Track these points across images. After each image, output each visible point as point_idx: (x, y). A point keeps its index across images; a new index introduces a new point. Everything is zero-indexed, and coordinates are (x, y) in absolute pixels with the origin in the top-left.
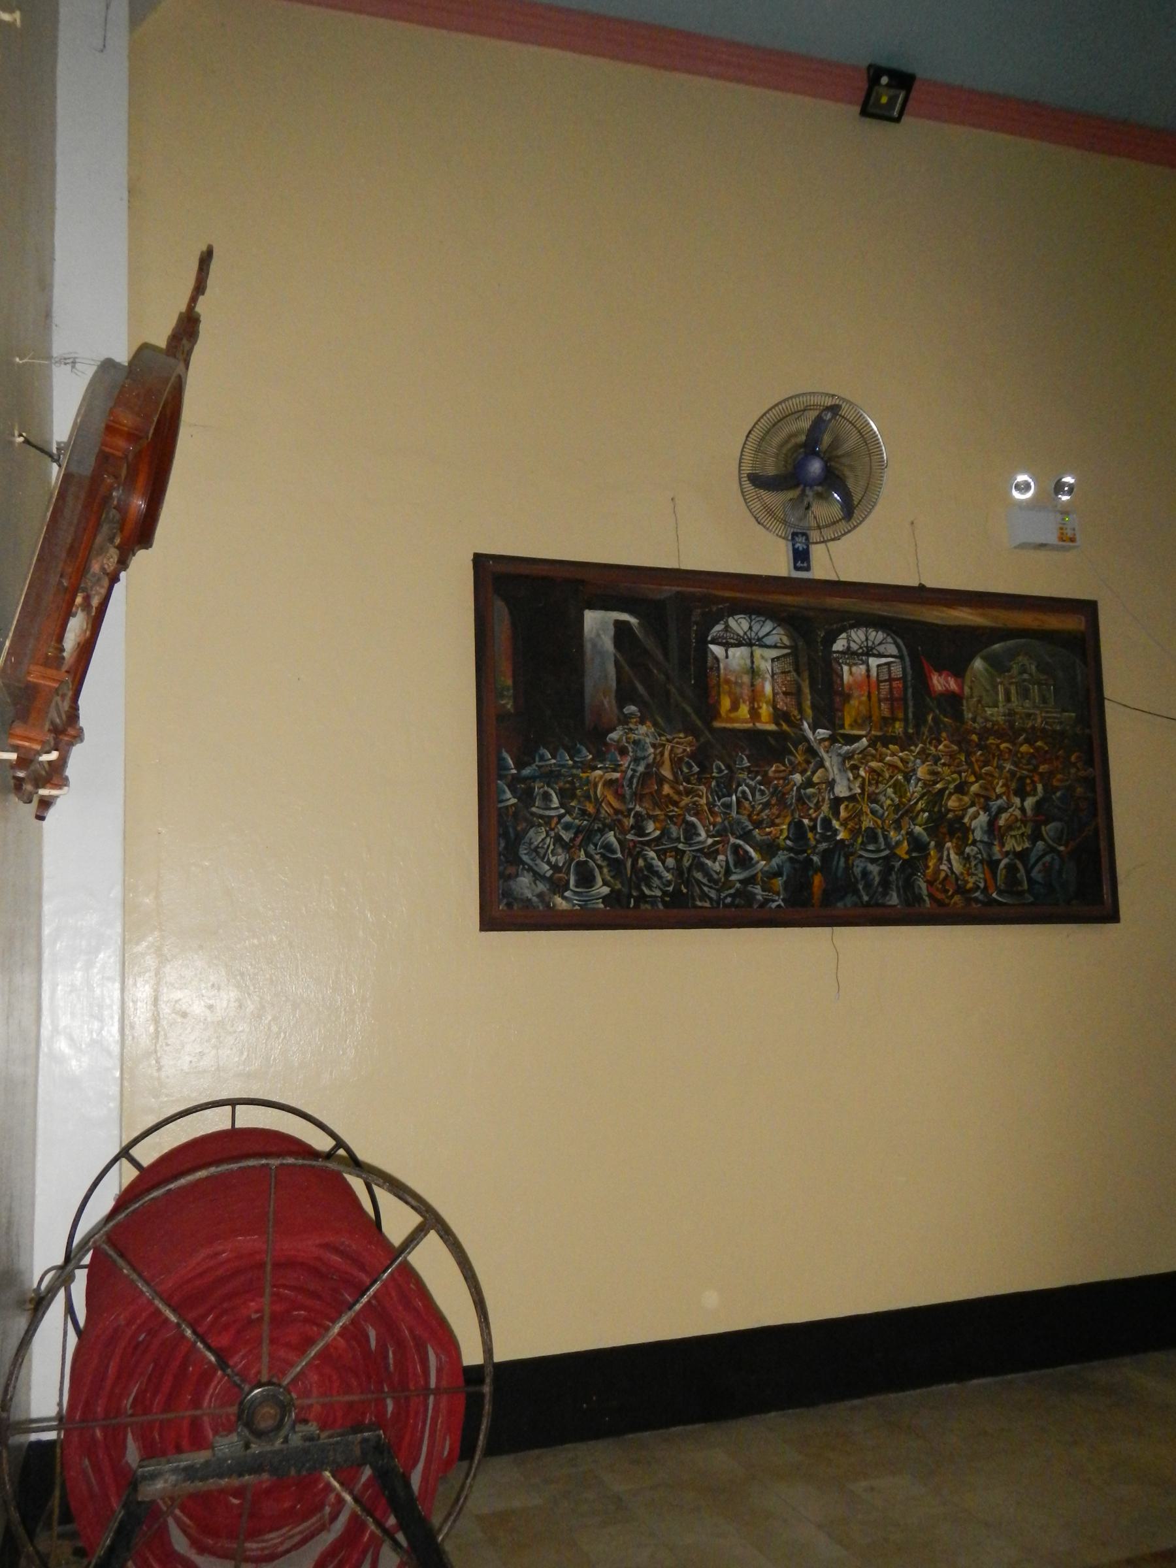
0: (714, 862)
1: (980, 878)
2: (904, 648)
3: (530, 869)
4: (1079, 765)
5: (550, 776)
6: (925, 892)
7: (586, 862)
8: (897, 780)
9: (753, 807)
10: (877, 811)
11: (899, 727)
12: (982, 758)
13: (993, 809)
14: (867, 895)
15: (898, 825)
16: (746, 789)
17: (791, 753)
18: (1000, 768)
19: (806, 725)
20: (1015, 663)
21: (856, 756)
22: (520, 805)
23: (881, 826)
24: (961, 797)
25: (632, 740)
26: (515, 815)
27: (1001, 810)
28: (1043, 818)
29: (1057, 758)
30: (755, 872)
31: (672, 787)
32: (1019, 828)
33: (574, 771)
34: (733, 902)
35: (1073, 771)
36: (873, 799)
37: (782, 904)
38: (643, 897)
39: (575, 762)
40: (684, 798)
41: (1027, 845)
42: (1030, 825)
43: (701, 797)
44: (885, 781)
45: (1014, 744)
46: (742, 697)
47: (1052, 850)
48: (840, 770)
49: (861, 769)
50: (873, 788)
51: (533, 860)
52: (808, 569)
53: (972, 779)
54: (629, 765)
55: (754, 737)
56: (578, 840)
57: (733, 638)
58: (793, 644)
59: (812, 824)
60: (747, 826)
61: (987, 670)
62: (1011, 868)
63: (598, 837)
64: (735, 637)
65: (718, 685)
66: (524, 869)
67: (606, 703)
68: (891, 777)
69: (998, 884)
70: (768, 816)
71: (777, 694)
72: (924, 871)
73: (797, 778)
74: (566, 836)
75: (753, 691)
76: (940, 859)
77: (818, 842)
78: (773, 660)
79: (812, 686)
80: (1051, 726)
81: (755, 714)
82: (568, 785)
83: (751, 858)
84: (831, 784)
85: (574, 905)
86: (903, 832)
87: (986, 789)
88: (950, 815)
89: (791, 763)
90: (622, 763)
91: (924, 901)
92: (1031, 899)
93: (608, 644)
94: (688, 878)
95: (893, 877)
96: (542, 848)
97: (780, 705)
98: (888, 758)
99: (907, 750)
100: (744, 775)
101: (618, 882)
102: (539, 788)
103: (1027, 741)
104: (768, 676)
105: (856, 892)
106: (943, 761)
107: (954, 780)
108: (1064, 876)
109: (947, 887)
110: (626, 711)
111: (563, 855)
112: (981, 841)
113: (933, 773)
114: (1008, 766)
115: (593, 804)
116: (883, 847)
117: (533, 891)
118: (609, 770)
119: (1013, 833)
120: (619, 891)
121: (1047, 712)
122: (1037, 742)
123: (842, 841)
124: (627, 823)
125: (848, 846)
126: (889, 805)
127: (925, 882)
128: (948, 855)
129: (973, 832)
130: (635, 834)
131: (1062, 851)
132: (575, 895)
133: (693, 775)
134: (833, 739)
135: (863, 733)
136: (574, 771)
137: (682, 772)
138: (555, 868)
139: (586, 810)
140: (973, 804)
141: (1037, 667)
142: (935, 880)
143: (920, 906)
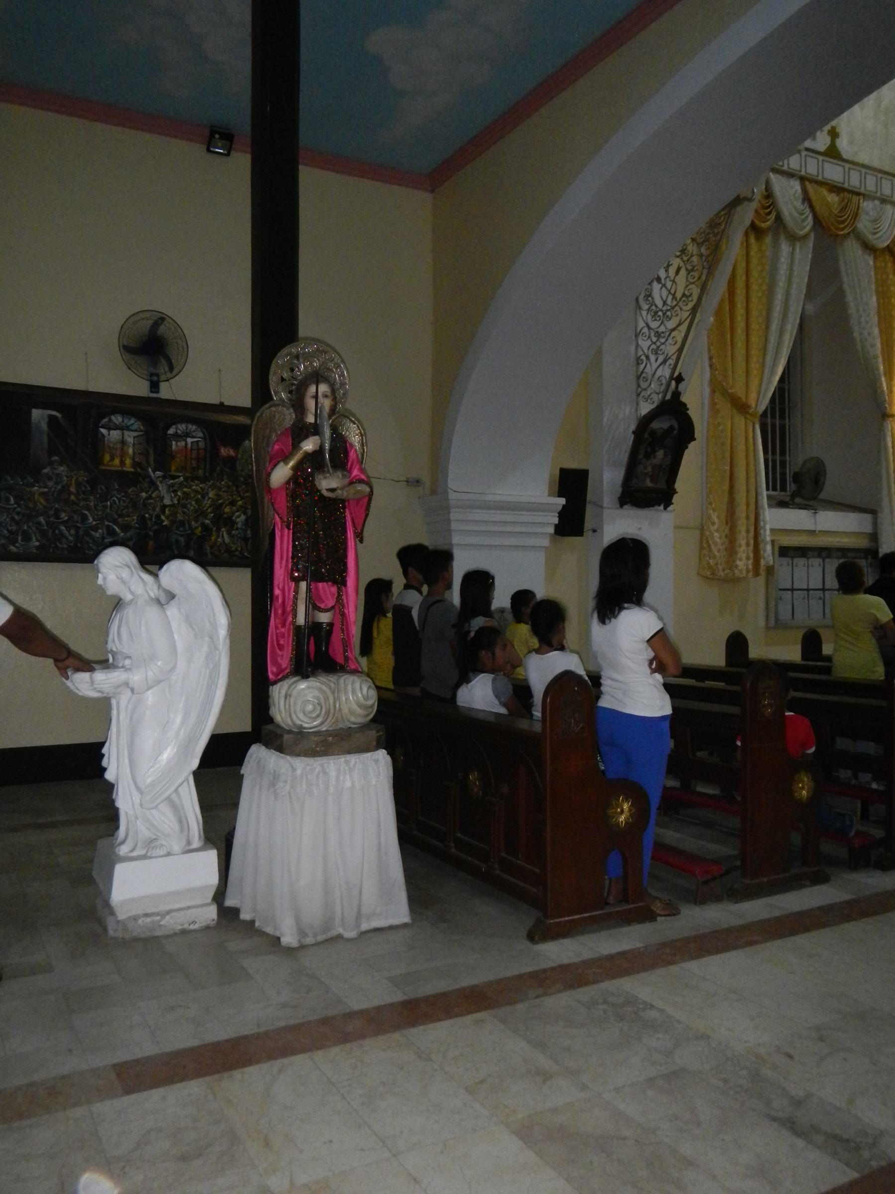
11: (201, 472)
16: (116, 499)
19: (150, 470)
21: (176, 486)
31: (76, 497)
33: (23, 487)
36: (184, 506)
43: (90, 502)
50: (184, 501)
52: (158, 392)
53: (239, 499)
55: (121, 475)
68: (195, 496)
73: (144, 495)
74: (16, 517)
78: (134, 437)
81: (122, 463)
84: (162, 499)
85: (20, 550)
88: (225, 516)
93: (44, 426)
97: (137, 459)
98: (194, 487)
100: (115, 492)
107: (229, 499)
113: (217, 495)
123: (166, 525)
128: (223, 535)
129: (237, 524)
134: (164, 477)
135: (181, 474)
138: (11, 532)
140: (238, 511)
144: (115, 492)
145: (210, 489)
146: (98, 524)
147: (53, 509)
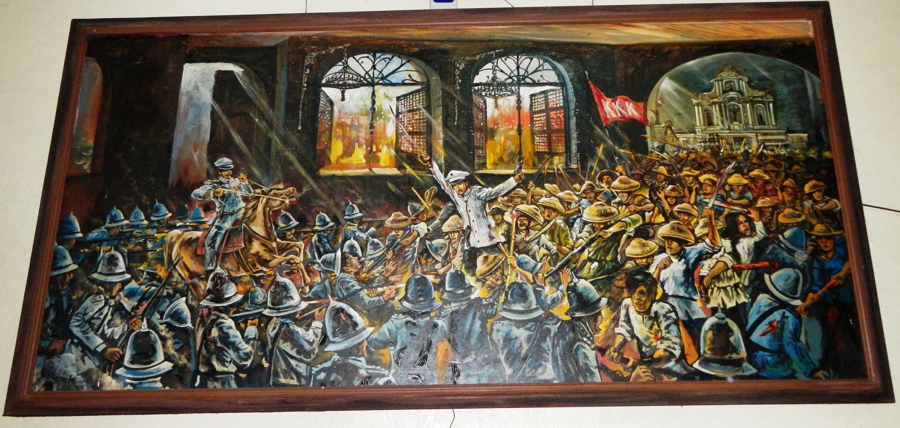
0: (307, 330)
1: (676, 343)
2: (565, 74)
3: (80, 343)
4: (816, 195)
5: (119, 239)
6: (593, 363)
8: (555, 225)
9: (362, 263)
11: (558, 163)
12: (673, 194)
13: (690, 256)
17: (419, 201)
18: (699, 204)
19: (436, 168)
20: (718, 81)
21: (500, 199)
22: (81, 271)
23: (532, 281)
24: (644, 241)
25: (221, 194)
26: (73, 281)
27: (702, 257)
28: (767, 263)
29: (783, 188)
30: (360, 341)
31: (263, 245)
32: (730, 279)
35: (808, 204)
36: (522, 248)
38: (212, 374)
39: (151, 222)
41: (743, 299)
43: (297, 254)
44: (539, 227)
45: (719, 174)
46: (358, 141)
47: (783, 305)
48: (478, 216)
51: (84, 332)
53: (661, 219)
56: (142, 309)
57: (352, 79)
58: (425, 80)
59: (438, 281)
60: (353, 286)
61: (677, 91)
62: (721, 330)
63: (166, 305)
64: (355, 77)
65: (330, 129)
66: (72, 343)
67: (195, 157)
68: (547, 222)
69: (702, 351)
70: (381, 273)
71: (402, 134)
73: (422, 228)
74: (128, 304)
75: (372, 133)
76: (616, 320)
78: (398, 99)
79: (446, 125)
80: (772, 150)
81: (372, 158)
82: (139, 247)
83: (355, 324)
84: (466, 233)
85: (126, 385)
87: (680, 231)
88: (629, 265)
89: (414, 210)
91: (592, 373)
92: (754, 371)
93: (206, 96)
95: (548, 344)
98: (543, 199)
99: (570, 189)
101: (183, 356)
103: (738, 170)
104: (392, 117)
106: (618, 199)
107: (634, 222)
109: (625, 356)
110: (217, 164)
111: (121, 326)
114: (712, 202)
115: (166, 267)
116: (534, 306)
117: (78, 370)
118: (190, 228)
119: (721, 285)
120: (185, 366)
121: (765, 134)
122: (752, 171)
123: (479, 300)
124: (203, 287)
125: (486, 306)
126: (544, 255)
127: (593, 349)
128: (627, 315)
129: (662, 286)
130: (212, 300)
131: (797, 306)
132: (128, 373)
133: (290, 230)
134: (470, 181)
135: (511, 172)
137: (277, 226)
138: (110, 341)
139: (156, 274)
140: (662, 250)
141: (749, 83)
142: (609, 347)
144: (354, 228)
145: (584, 201)
146: (314, 306)
147: (211, 276)
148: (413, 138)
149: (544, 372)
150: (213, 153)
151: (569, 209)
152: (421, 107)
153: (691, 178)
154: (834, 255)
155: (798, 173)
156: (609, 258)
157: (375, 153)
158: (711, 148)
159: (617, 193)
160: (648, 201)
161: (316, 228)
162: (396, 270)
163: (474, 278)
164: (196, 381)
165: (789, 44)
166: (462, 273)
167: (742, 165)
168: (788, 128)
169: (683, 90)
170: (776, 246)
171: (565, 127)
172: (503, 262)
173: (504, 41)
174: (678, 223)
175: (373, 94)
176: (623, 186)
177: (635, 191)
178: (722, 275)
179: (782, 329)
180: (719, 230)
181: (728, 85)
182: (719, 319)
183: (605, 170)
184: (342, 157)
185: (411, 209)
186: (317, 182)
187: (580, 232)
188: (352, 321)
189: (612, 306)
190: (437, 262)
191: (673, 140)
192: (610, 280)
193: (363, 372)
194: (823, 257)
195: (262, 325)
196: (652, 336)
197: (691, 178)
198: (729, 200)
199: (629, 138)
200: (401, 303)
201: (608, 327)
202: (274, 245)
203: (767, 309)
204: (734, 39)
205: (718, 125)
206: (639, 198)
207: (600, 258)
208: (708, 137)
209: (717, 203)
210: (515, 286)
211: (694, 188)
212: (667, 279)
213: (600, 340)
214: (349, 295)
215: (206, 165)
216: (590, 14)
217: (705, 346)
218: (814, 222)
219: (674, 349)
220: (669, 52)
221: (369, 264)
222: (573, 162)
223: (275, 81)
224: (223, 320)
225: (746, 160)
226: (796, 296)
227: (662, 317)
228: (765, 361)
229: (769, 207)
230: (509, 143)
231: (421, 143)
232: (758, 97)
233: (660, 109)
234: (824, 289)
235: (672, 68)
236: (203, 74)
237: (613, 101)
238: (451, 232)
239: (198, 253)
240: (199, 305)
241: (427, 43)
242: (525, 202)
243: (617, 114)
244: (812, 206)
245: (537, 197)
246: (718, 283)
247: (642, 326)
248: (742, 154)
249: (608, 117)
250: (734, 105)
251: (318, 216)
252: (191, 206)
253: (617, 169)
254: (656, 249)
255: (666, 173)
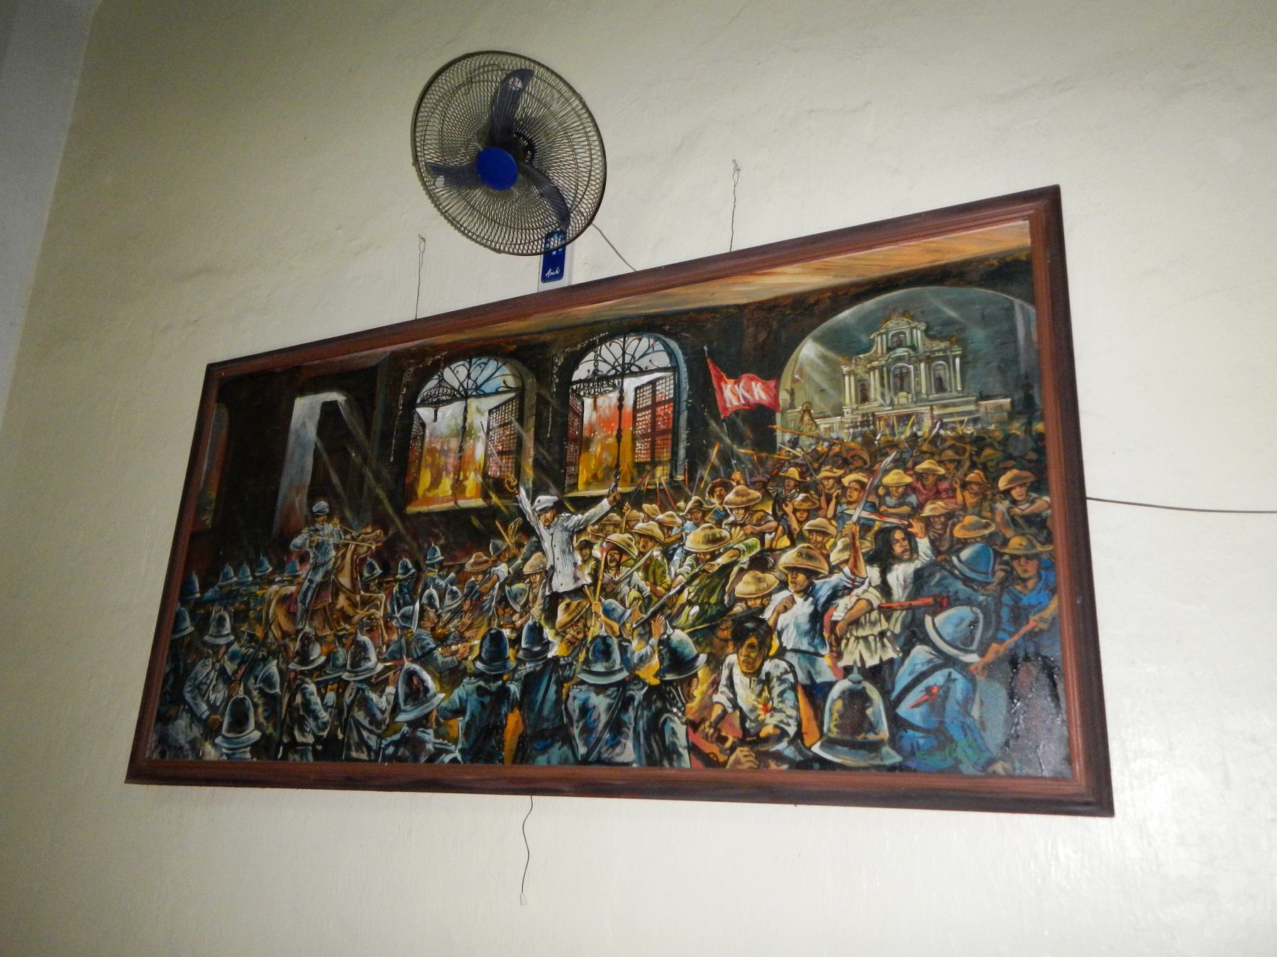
0: (381, 696)
1: (790, 717)
5: (228, 597)
6: (682, 741)
7: (243, 700)
8: (651, 558)
10: (614, 609)
11: (661, 474)
12: (805, 506)
13: (821, 593)
14: (586, 743)
15: (646, 628)
16: (434, 592)
18: (840, 517)
20: (881, 334)
21: (589, 529)
23: (618, 633)
24: (760, 574)
26: (190, 644)
27: (835, 594)
28: (930, 600)
29: (964, 486)
30: (429, 710)
31: (349, 599)
32: (873, 624)
33: (253, 589)
34: (396, 752)
35: (1002, 506)
36: (610, 591)
37: (459, 758)
38: (293, 745)
39: (255, 577)
40: (358, 611)
41: (890, 653)
42: (899, 616)
43: (378, 608)
44: (632, 562)
45: (871, 472)
46: (446, 469)
47: (949, 661)
48: (564, 552)
49: (596, 547)
51: (194, 698)
53: (785, 542)
54: (307, 575)
55: (456, 518)
56: (240, 672)
57: (446, 395)
59: (514, 635)
60: (428, 644)
61: (824, 358)
62: (856, 698)
63: (261, 668)
68: (642, 554)
69: (825, 729)
70: (456, 628)
71: (491, 455)
72: (684, 705)
73: (503, 570)
74: (230, 667)
75: (460, 458)
76: (715, 684)
77: (520, 662)
78: (490, 412)
79: (538, 439)
80: (953, 429)
81: (458, 487)
82: (243, 606)
83: (427, 690)
84: (548, 574)
86: (654, 641)
87: (810, 557)
88: (738, 608)
89: (496, 548)
90: (300, 573)
91: (680, 755)
93: (311, 432)
94: (346, 720)
95: (630, 715)
96: (205, 683)
97: (494, 471)
98: (640, 525)
99: (673, 509)
100: (433, 574)
101: (270, 725)
102: (216, 613)
103: (899, 463)
104: (482, 435)
105: (568, 740)
106: (731, 519)
107: (750, 548)
108: (975, 712)
109: (723, 734)
112: (796, 651)
117: (187, 736)
118: (286, 583)
119: (861, 633)
120: (271, 734)
121: (945, 406)
123: (556, 659)
124: (292, 649)
125: (564, 667)
126: (635, 599)
127: (683, 723)
128: (730, 678)
129: (780, 635)
131: (970, 664)
134: (558, 508)
135: (605, 491)
136: (253, 589)
137: (362, 576)
138: (213, 708)
140: (783, 585)
141: (926, 332)
142: (703, 720)
143: (671, 764)
145: (689, 524)
148: (502, 459)
149: (622, 753)
150: (313, 497)
151: (670, 537)
152: (513, 419)
153: (831, 481)
154: (1036, 583)
155: (992, 460)
156: (713, 600)
157: (462, 481)
158: (863, 435)
159: (731, 510)
160: (771, 518)
161: (398, 576)
162: (472, 623)
163: (553, 632)
164: (278, 752)
165: (995, 262)
166: (540, 625)
167: (906, 456)
168: (981, 393)
169: (831, 355)
170: (946, 573)
171: (674, 423)
172: (587, 610)
173: (609, 321)
174: (808, 547)
175: (466, 410)
176: (739, 499)
177: (753, 506)
178: (862, 619)
179: (946, 697)
180: (863, 554)
181: (895, 339)
182: (853, 682)
183: (719, 480)
184: (429, 489)
185: (493, 548)
186: (403, 522)
187: (681, 566)
188: (423, 685)
189: (712, 666)
190: (515, 612)
191: (810, 429)
192: (712, 629)
193: (430, 747)
194: (1019, 588)
195: (340, 691)
196: (760, 706)
197: (831, 481)
198: (883, 508)
199: (753, 429)
200: (474, 664)
201: (704, 694)
202: (358, 598)
203: (925, 668)
204: (908, 269)
205: (876, 400)
206: (760, 514)
207: (702, 601)
208: (860, 419)
209: (865, 514)
210: (598, 640)
211: (834, 495)
212: (787, 626)
213: (694, 710)
214: (424, 655)
215: (305, 510)
216: (712, 267)
217: (830, 722)
218: (1009, 533)
219: (788, 724)
220: (816, 303)
221: (446, 617)
222: (679, 472)
223: (373, 408)
224: (307, 686)
225: (912, 448)
226: (971, 648)
227: (775, 680)
228: (915, 745)
229: (942, 515)
230: (605, 455)
231: (510, 465)
232: (939, 351)
233: (796, 386)
234: (1016, 638)
235: (818, 325)
236: (312, 408)
237: (735, 383)
238: (532, 574)
239: (292, 610)
240: (288, 669)
241: (525, 338)
242: (618, 531)
243: (739, 401)
244: (1008, 510)
245: (632, 523)
246: (857, 630)
247: (749, 692)
248: (907, 440)
249: (728, 405)
250: (901, 368)
251: (401, 562)
252: (289, 559)
253: (733, 477)
254: (776, 585)
255: (797, 477)
